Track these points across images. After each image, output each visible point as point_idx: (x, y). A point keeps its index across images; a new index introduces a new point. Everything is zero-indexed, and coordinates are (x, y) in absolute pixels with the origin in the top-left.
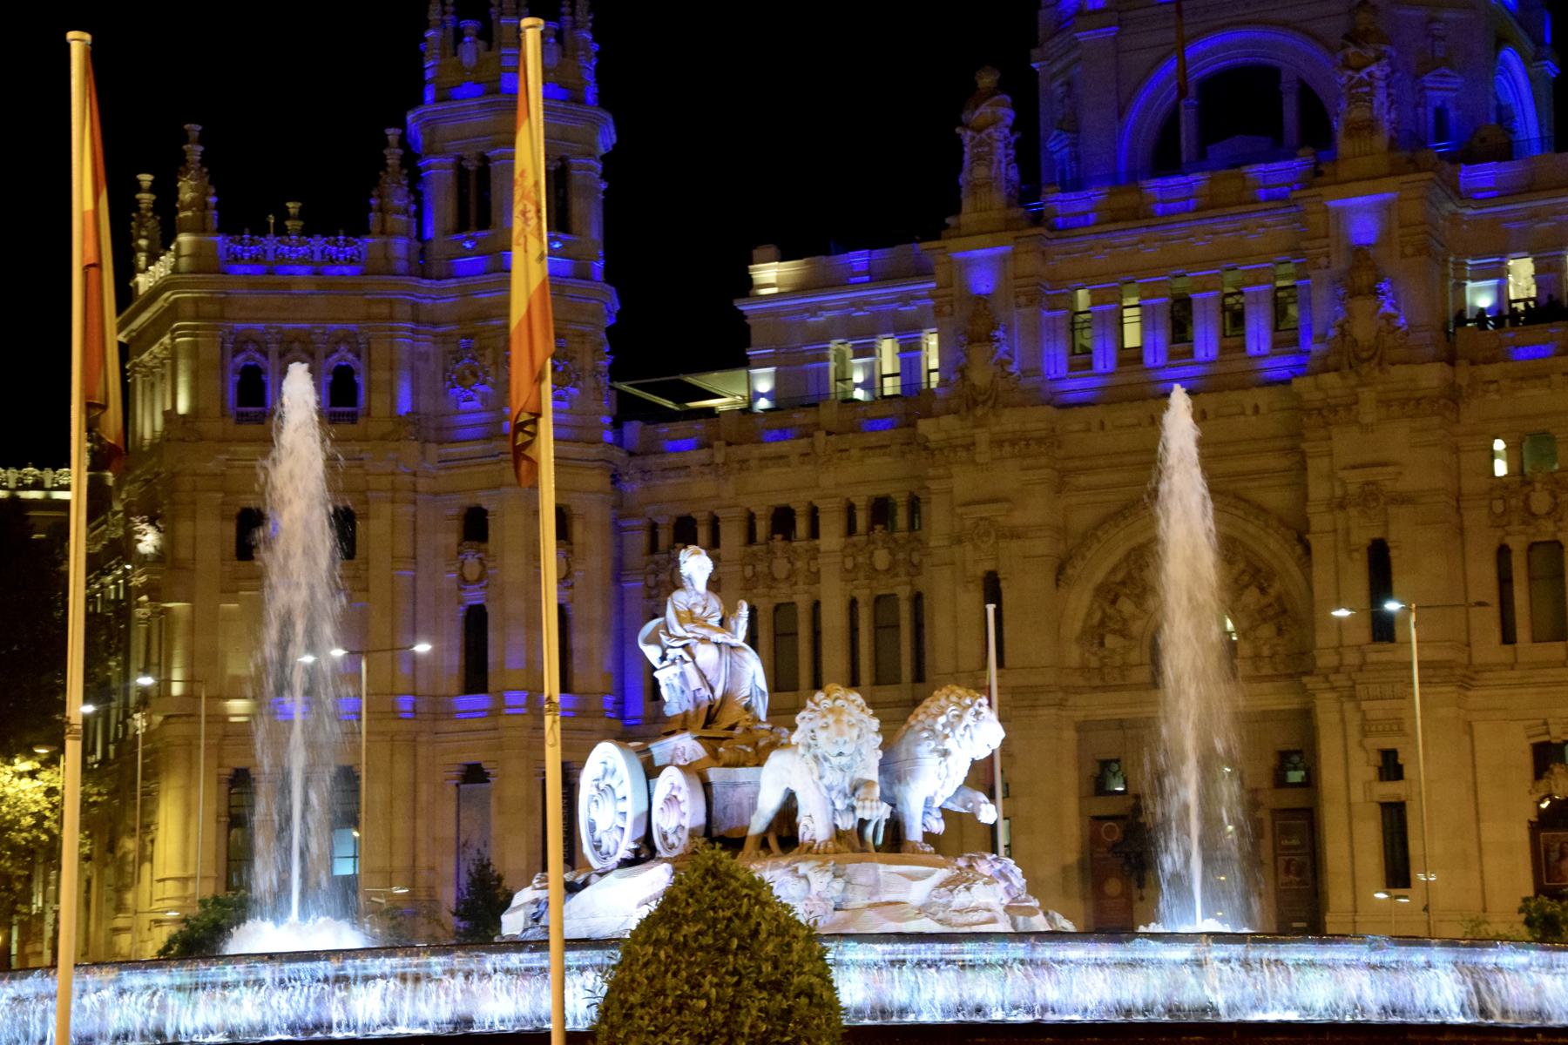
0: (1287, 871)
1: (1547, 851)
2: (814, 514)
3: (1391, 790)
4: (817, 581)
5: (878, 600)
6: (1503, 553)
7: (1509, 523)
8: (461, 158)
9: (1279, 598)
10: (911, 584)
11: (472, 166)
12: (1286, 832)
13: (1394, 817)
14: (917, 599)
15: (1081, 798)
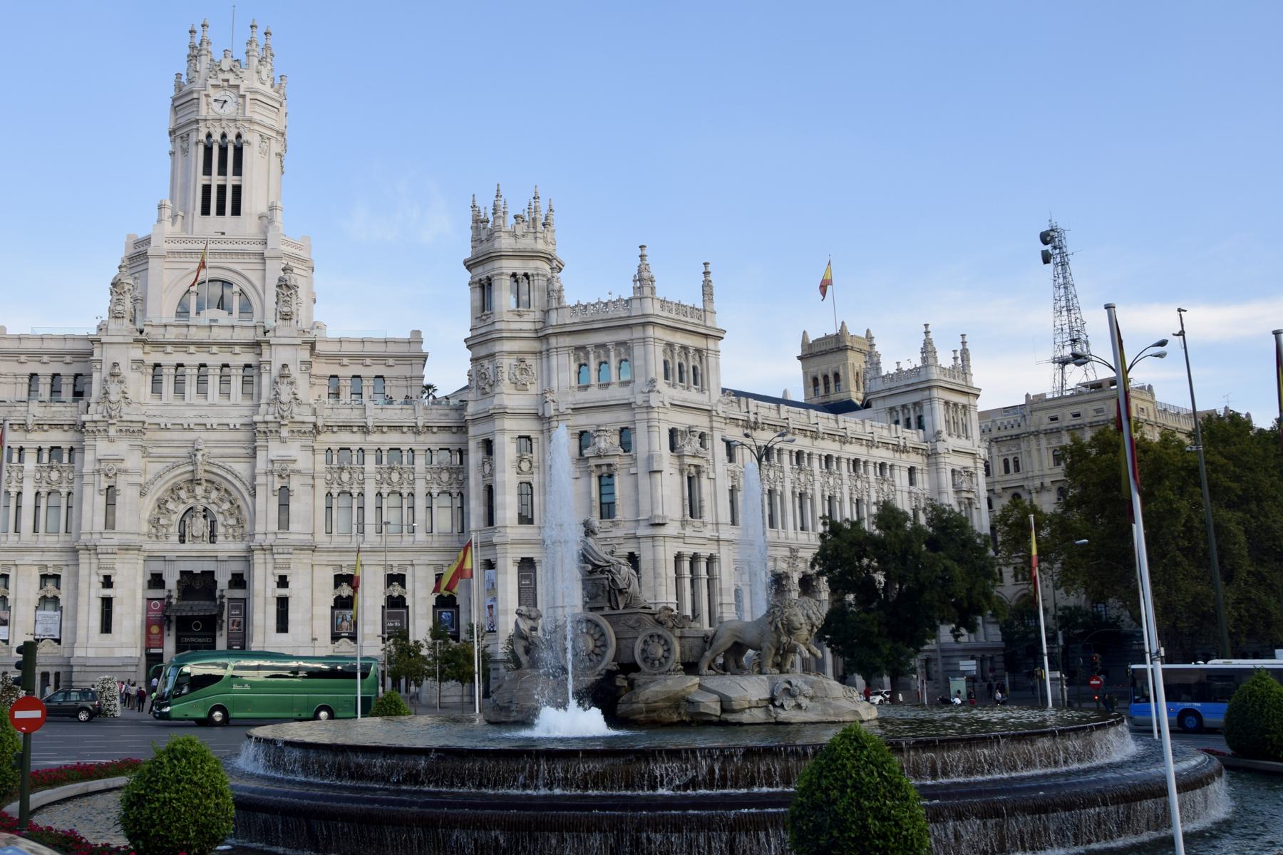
0: (233, 625)
1: (337, 618)
3: (283, 592)
12: (234, 608)
13: (283, 603)
15: (143, 590)
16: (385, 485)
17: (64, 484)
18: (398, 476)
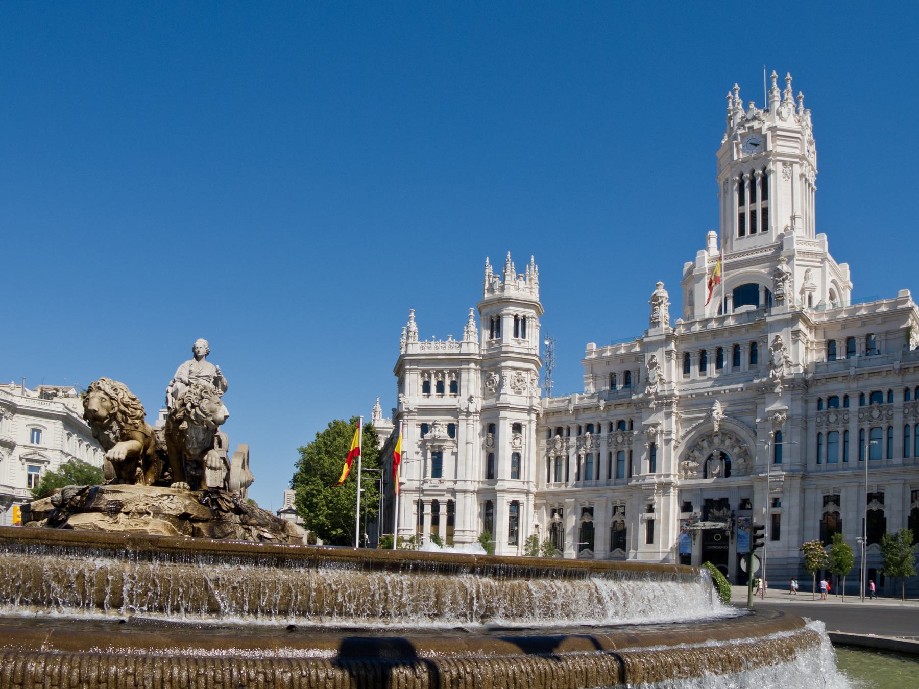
2: (599, 426)
4: (600, 446)
5: (619, 452)
6: (819, 434)
7: (822, 425)
8: (491, 317)
9: (746, 450)
10: (629, 447)
11: (495, 319)
14: (631, 452)
16: (867, 422)
17: (626, 445)
18: (873, 414)
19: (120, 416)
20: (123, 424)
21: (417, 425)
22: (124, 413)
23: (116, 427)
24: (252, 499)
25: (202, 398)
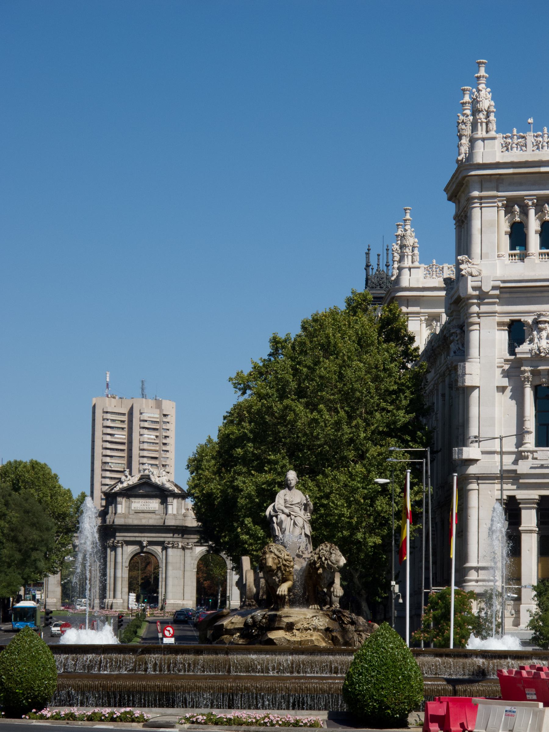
19: (283, 567)
20: (284, 572)
21: (500, 324)
22: (285, 565)
23: (280, 574)
24: (42, 462)
25: (331, 553)
